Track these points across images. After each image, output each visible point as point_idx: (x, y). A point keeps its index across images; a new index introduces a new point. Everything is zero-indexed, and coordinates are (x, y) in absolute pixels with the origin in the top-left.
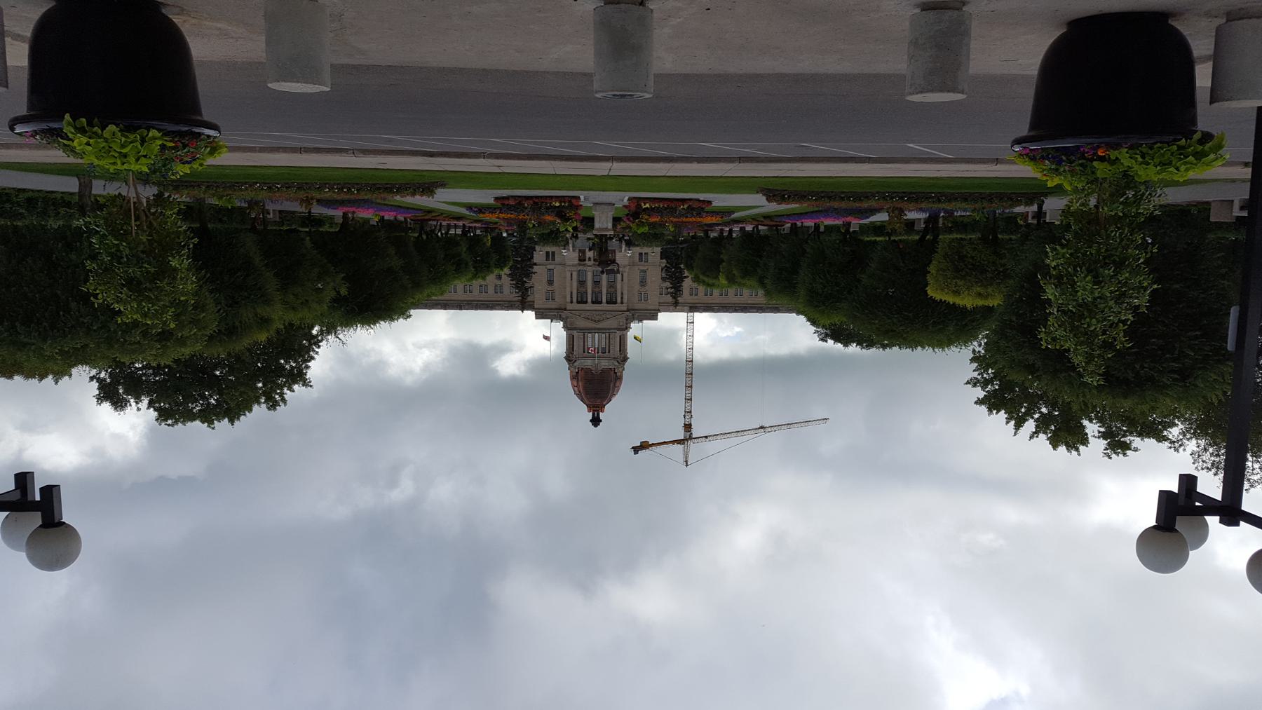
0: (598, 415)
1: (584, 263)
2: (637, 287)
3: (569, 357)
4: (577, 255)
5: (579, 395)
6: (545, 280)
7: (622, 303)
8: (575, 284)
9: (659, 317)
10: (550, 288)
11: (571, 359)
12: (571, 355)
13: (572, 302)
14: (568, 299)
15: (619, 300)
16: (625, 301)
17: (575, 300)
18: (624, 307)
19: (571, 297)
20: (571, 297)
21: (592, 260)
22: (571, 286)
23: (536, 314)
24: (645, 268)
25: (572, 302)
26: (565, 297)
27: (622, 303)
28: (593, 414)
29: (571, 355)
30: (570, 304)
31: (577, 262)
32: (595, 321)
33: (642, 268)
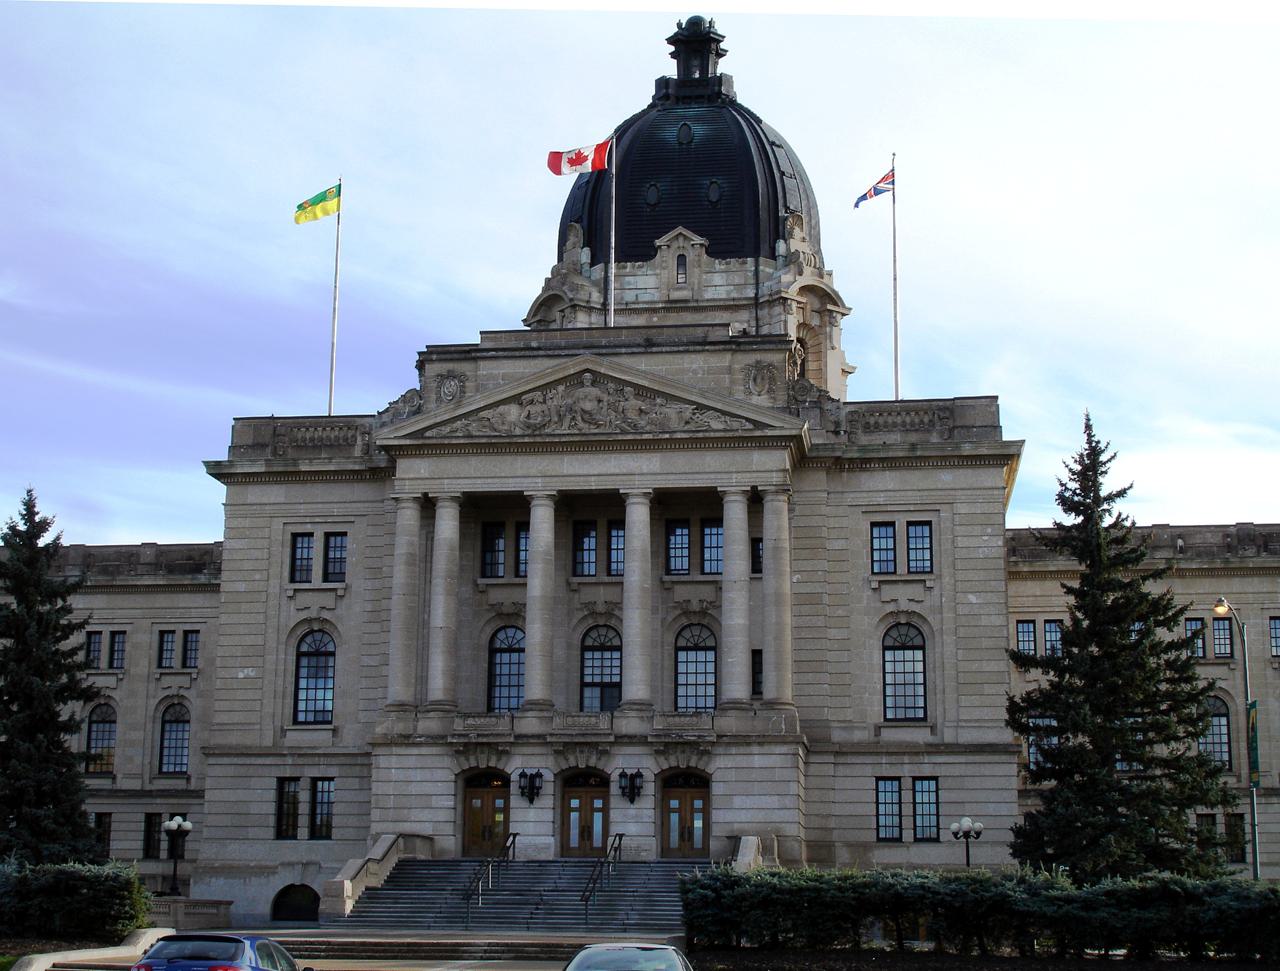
0: (684, 68)
1: (673, 761)
2: (350, 619)
3: (821, 312)
4: (717, 816)
5: (769, 145)
6: (945, 647)
7: (427, 506)
8: (735, 616)
9: (227, 441)
10: (903, 596)
11: (811, 302)
12: (815, 321)
13: (755, 500)
14: (778, 519)
15: (448, 523)
16: (409, 516)
17: (736, 513)
18: (415, 475)
19: (756, 543)
20: (756, 543)
21: (614, 789)
22: (756, 610)
23: (997, 428)
24: (296, 738)
25: (755, 500)
26: (807, 542)
27: (427, 506)
28: (704, 70)
29: (815, 321)
30: (761, 481)
31: (722, 767)
32: (598, 379)
33: (320, 738)
